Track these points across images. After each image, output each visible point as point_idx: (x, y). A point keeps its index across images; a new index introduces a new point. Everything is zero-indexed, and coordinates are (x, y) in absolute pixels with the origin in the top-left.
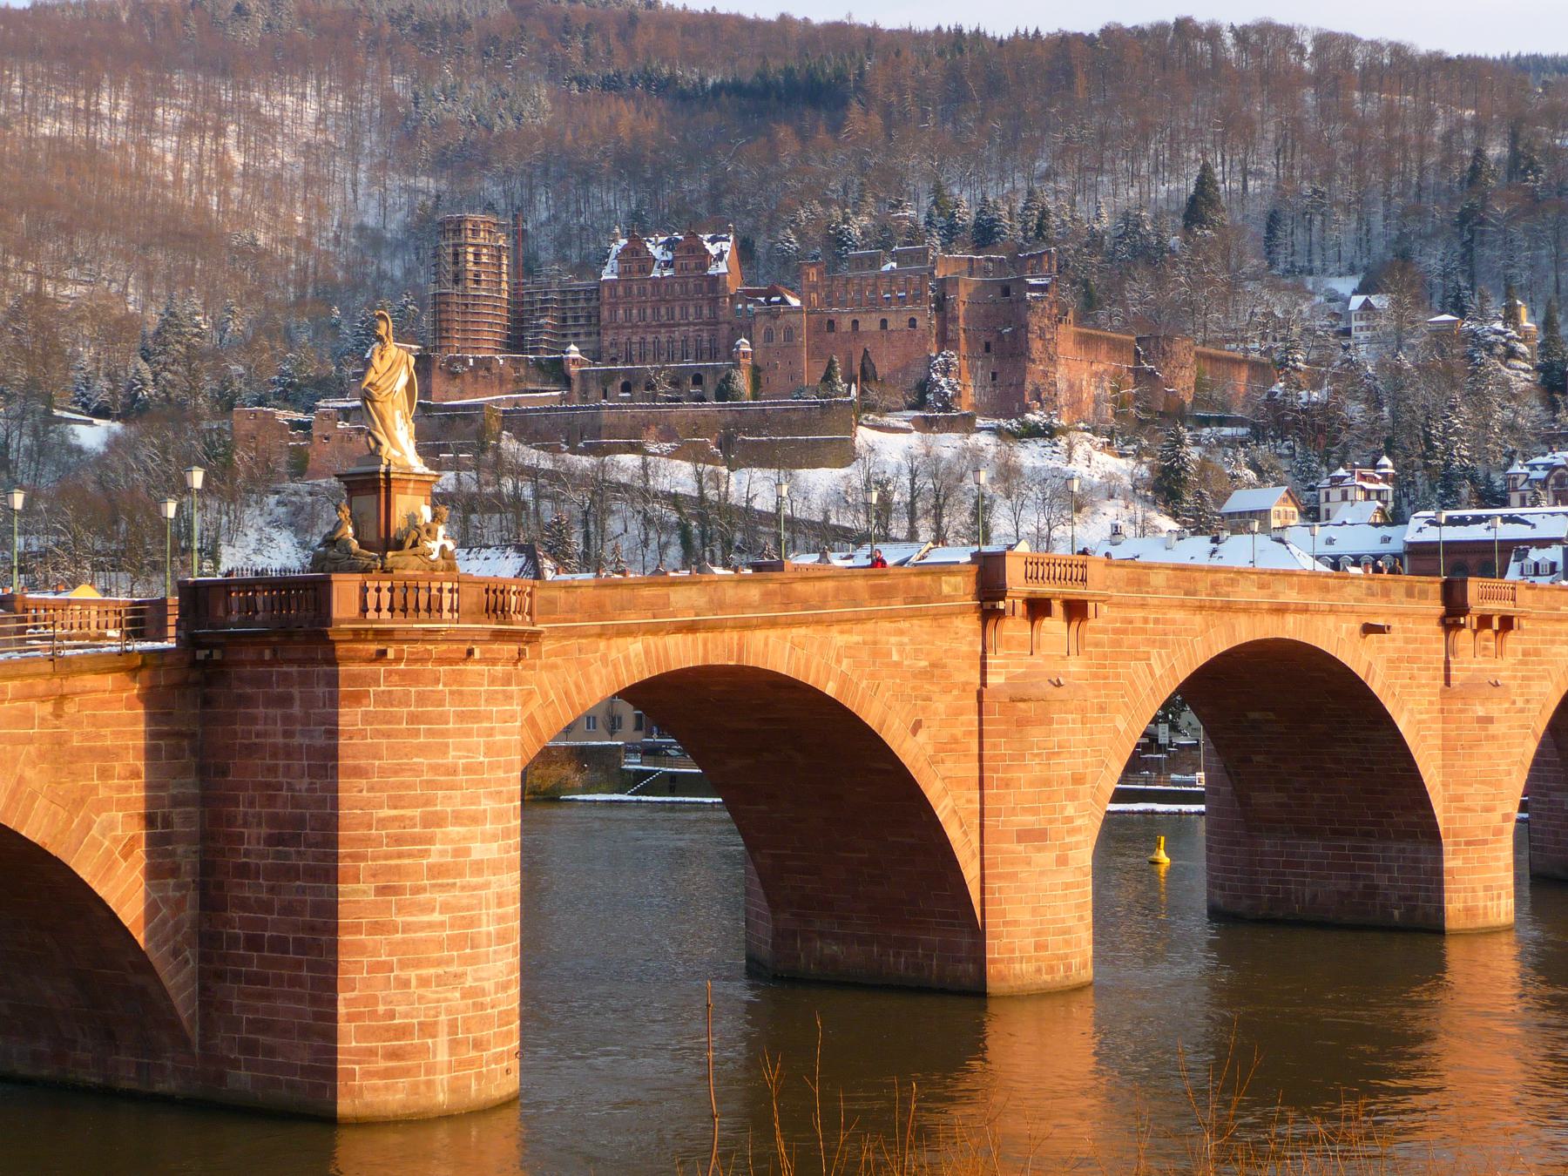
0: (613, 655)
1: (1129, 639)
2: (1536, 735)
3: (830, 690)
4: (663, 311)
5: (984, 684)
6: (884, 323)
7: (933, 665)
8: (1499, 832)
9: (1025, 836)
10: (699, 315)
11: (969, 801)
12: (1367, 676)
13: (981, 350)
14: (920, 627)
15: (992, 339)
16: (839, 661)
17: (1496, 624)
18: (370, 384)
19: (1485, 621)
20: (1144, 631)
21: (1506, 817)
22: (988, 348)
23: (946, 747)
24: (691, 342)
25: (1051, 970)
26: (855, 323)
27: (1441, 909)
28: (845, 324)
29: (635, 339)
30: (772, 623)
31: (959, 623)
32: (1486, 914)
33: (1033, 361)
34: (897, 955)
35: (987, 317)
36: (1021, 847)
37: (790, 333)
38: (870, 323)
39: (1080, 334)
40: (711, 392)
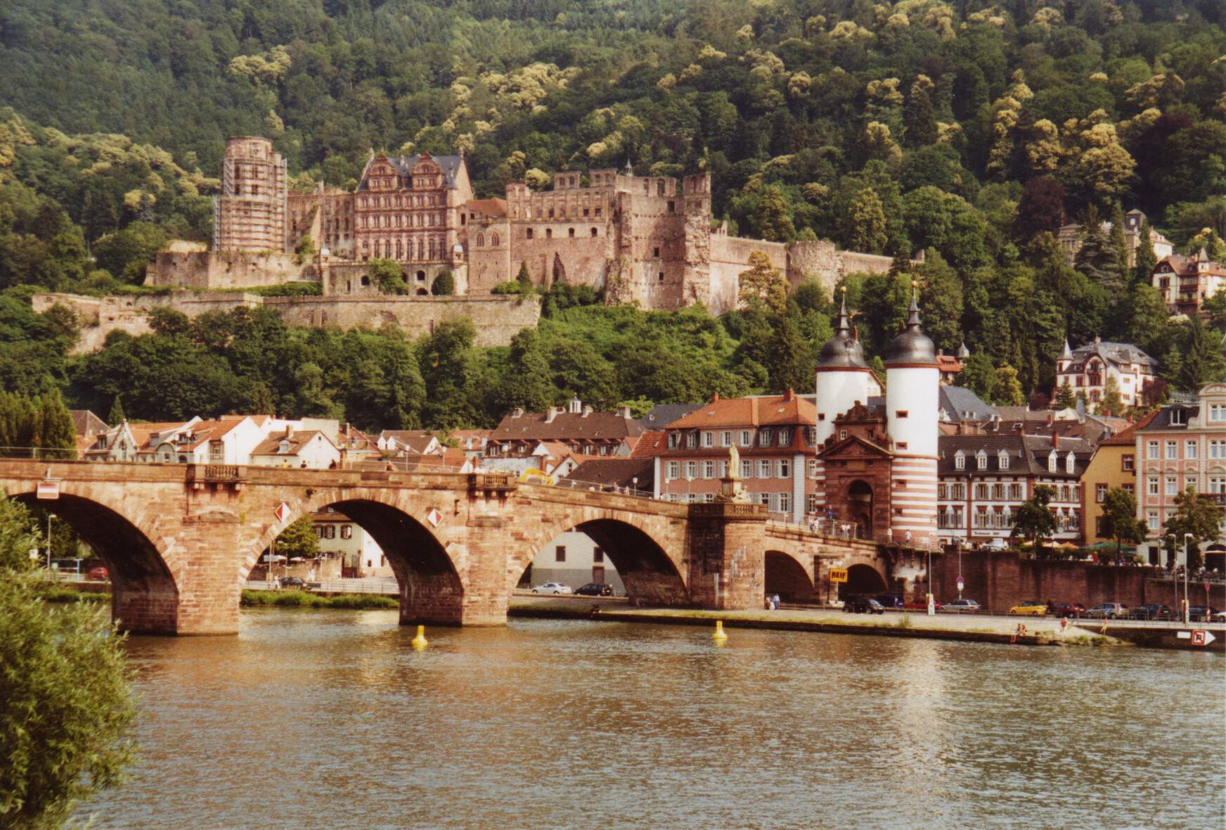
6: (572, 231)
10: (432, 222)
13: (651, 254)
15: (660, 246)
22: (656, 252)
26: (549, 231)
28: (540, 231)
33: (689, 264)
37: (496, 241)
39: (735, 242)
40: (429, 289)
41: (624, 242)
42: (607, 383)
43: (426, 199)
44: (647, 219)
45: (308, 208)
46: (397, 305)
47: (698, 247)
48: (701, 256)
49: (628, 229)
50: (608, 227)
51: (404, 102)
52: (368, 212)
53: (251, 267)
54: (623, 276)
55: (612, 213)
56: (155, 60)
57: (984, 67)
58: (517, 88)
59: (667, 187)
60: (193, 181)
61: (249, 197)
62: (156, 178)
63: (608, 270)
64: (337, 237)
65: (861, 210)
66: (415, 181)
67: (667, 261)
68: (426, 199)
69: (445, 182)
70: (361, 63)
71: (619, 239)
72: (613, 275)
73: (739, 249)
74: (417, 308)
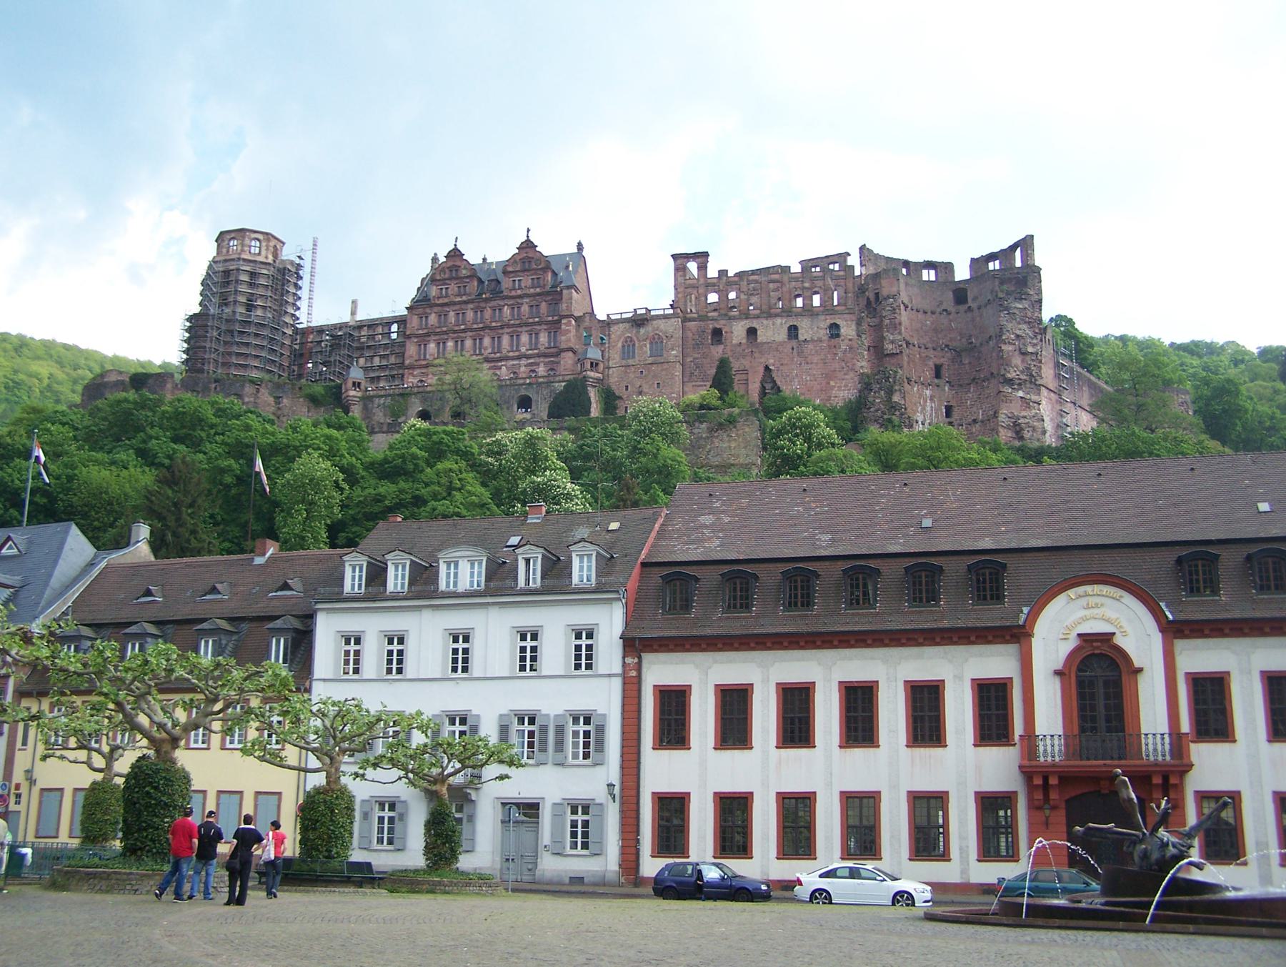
4: (487, 341)
6: (793, 331)
13: (929, 374)
15: (944, 360)
26: (752, 332)
28: (738, 331)
33: (1009, 382)
35: (936, 331)
38: (773, 331)
43: (525, 308)
44: (920, 315)
49: (895, 326)
50: (859, 324)
52: (428, 335)
54: (896, 398)
55: (863, 302)
66: (506, 283)
68: (525, 308)
71: (878, 350)
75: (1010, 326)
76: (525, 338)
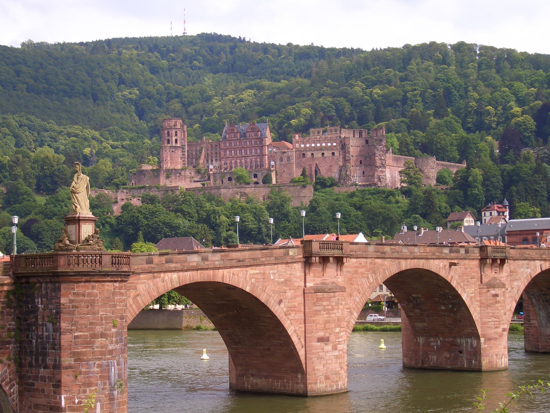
0: (166, 278)
1: (360, 270)
2: (515, 301)
3: (248, 289)
4: (243, 151)
5: (305, 286)
6: (323, 154)
7: (286, 280)
8: (501, 336)
9: (320, 340)
11: (301, 328)
12: (451, 281)
13: (358, 163)
14: (281, 267)
15: (362, 159)
16: (251, 279)
17: (499, 261)
18: (73, 187)
19: (494, 260)
20: (365, 267)
21: (504, 330)
22: (361, 162)
23: (291, 309)
24: (254, 162)
25: (331, 386)
26: (313, 154)
27: (480, 362)
28: (309, 154)
29: (233, 162)
30: (226, 268)
31: (295, 265)
32: (497, 364)
34: (278, 382)
36: (319, 344)
37: (289, 158)
38: (318, 155)
39: (394, 157)
41: (347, 158)
42: (360, 221)
43: (253, 142)
45: (198, 148)
46: (248, 189)
47: (381, 159)
48: (382, 164)
49: (349, 152)
50: (340, 152)
51: (191, 109)
53: (178, 175)
54: (348, 173)
55: (341, 146)
56: (85, 95)
57: (453, 85)
58: (241, 100)
59: (363, 134)
60: (108, 144)
61: (174, 145)
62: (94, 142)
63: (340, 171)
64: (212, 161)
65: (440, 143)
66: (248, 135)
67: (366, 166)
68: (253, 142)
69: (261, 135)
70: (169, 93)
71: (344, 158)
72: (343, 173)
73: (397, 160)
74: (257, 190)
75: (377, 152)
76: (253, 151)
